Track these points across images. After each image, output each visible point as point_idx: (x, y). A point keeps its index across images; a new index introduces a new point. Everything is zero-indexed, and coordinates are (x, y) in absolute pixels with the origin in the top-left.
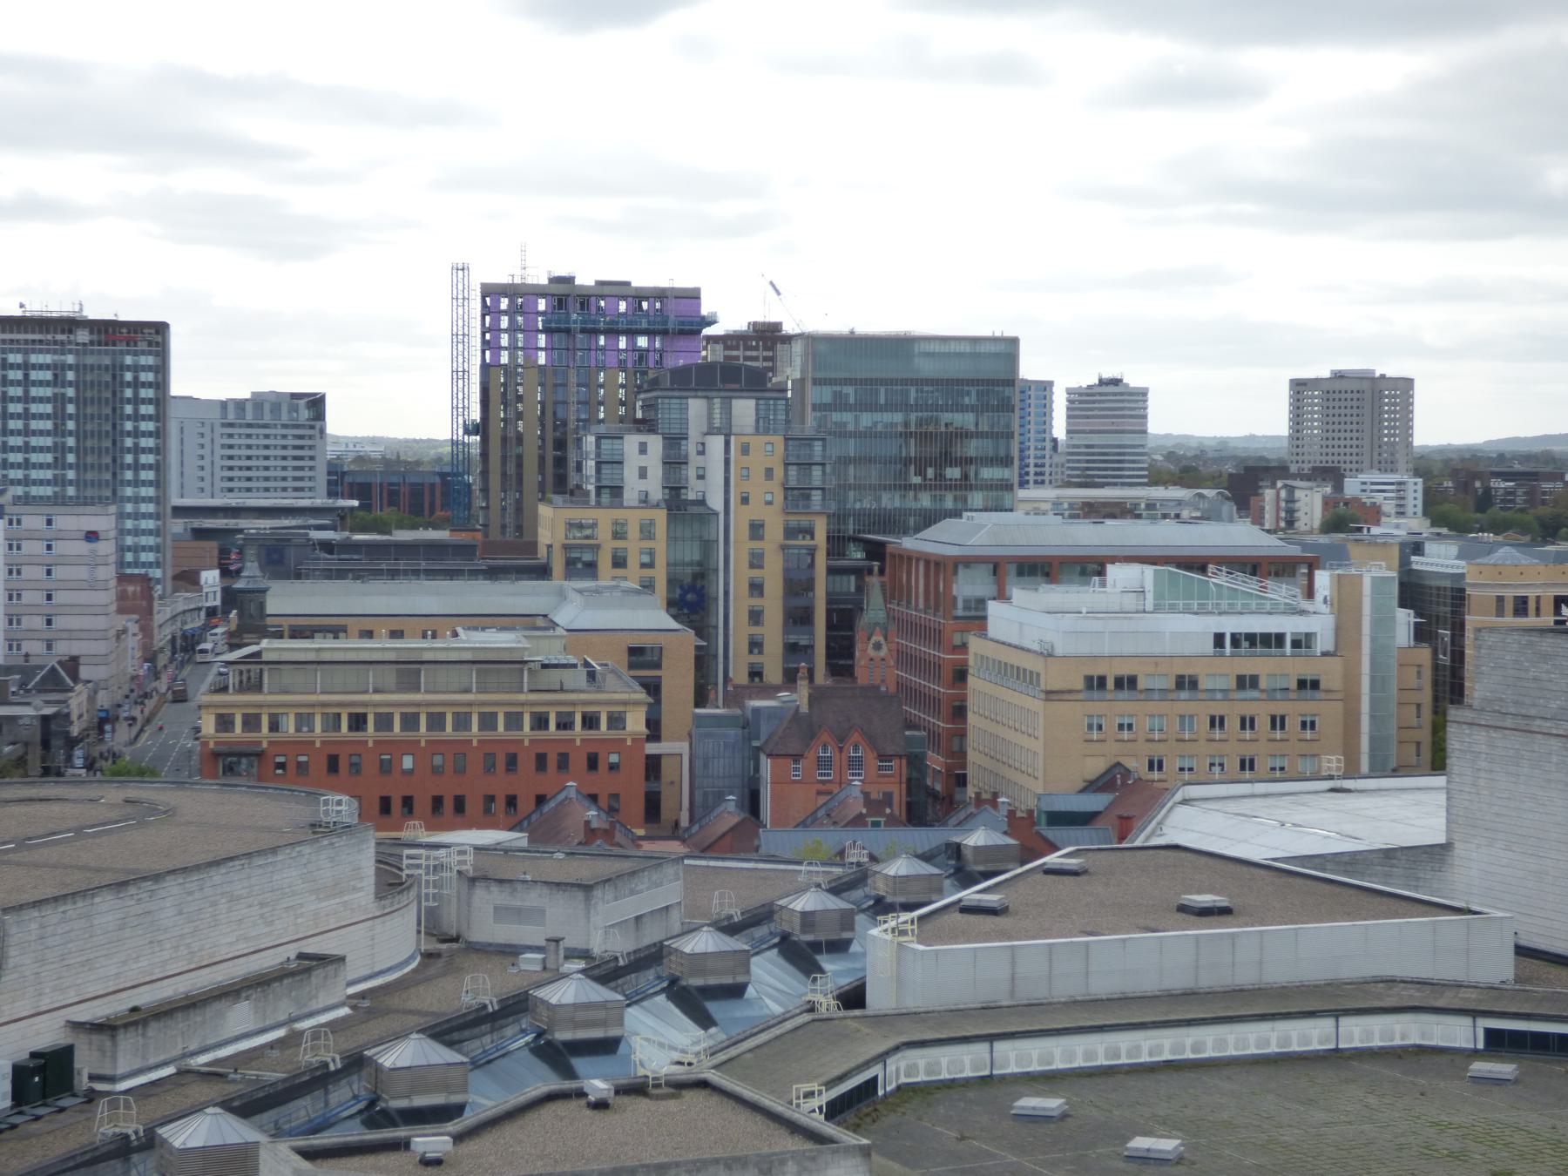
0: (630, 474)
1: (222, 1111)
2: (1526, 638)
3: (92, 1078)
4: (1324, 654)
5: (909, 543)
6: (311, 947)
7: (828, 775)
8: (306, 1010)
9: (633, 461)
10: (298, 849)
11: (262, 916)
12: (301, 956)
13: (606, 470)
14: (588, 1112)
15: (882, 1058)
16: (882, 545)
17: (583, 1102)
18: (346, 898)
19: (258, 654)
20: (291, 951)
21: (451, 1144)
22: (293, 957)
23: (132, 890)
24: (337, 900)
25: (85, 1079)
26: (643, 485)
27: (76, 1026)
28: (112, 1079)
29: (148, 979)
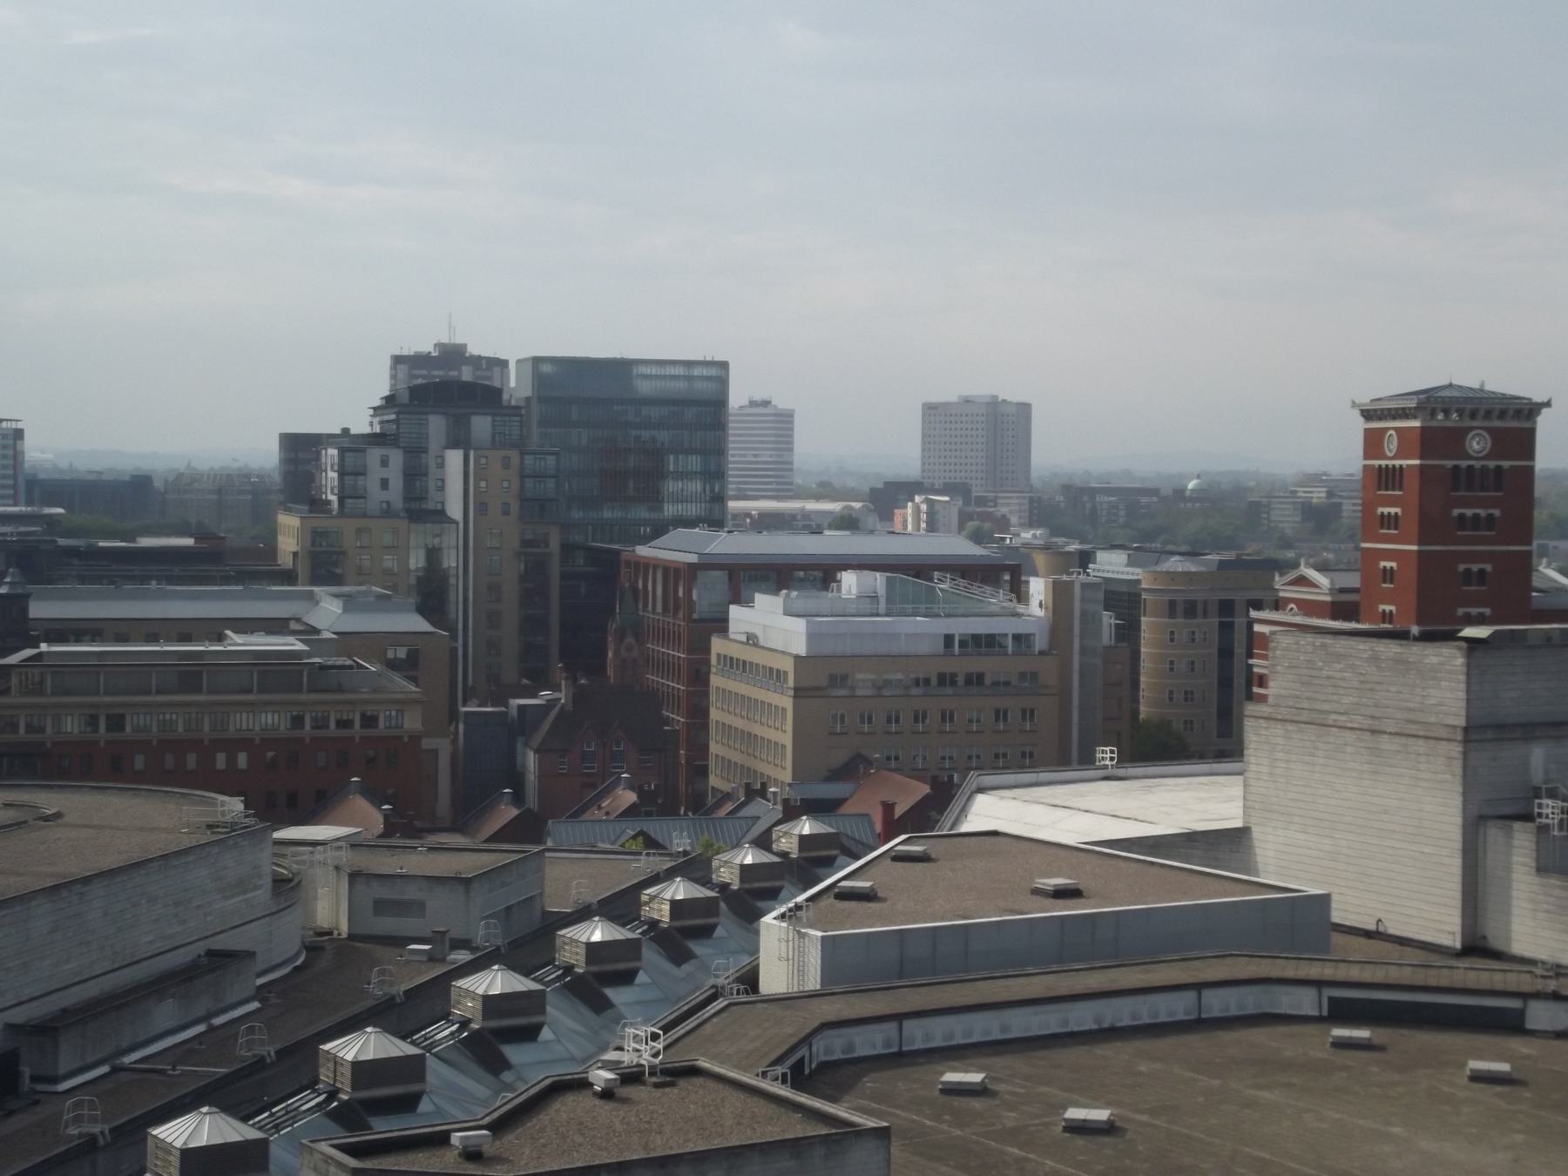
0: (372, 483)
1: (217, 1110)
2: (1321, 640)
3: (35, 1079)
4: (1041, 653)
5: (643, 551)
6: (219, 943)
7: (593, 768)
8: (222, 1005)
9: (375, 473)
10: (207, 849)
11: (176, 915)
12: (211, 953)
13: (349, 480)
14: (597, 1102)
15: (807, 1040)
16: (617, 553)
17: (588, 1092)
18: (249, 895)
19: (40, 655)
20: (200, 948)
21: (491, 1138)
22: (202, 953)
23: (64, 893)
24: (241, 898)
25: (27, 1080)
26: (385, 496)
27: (12, 1028)
28: (56, 1080)
29: (76, 980)
